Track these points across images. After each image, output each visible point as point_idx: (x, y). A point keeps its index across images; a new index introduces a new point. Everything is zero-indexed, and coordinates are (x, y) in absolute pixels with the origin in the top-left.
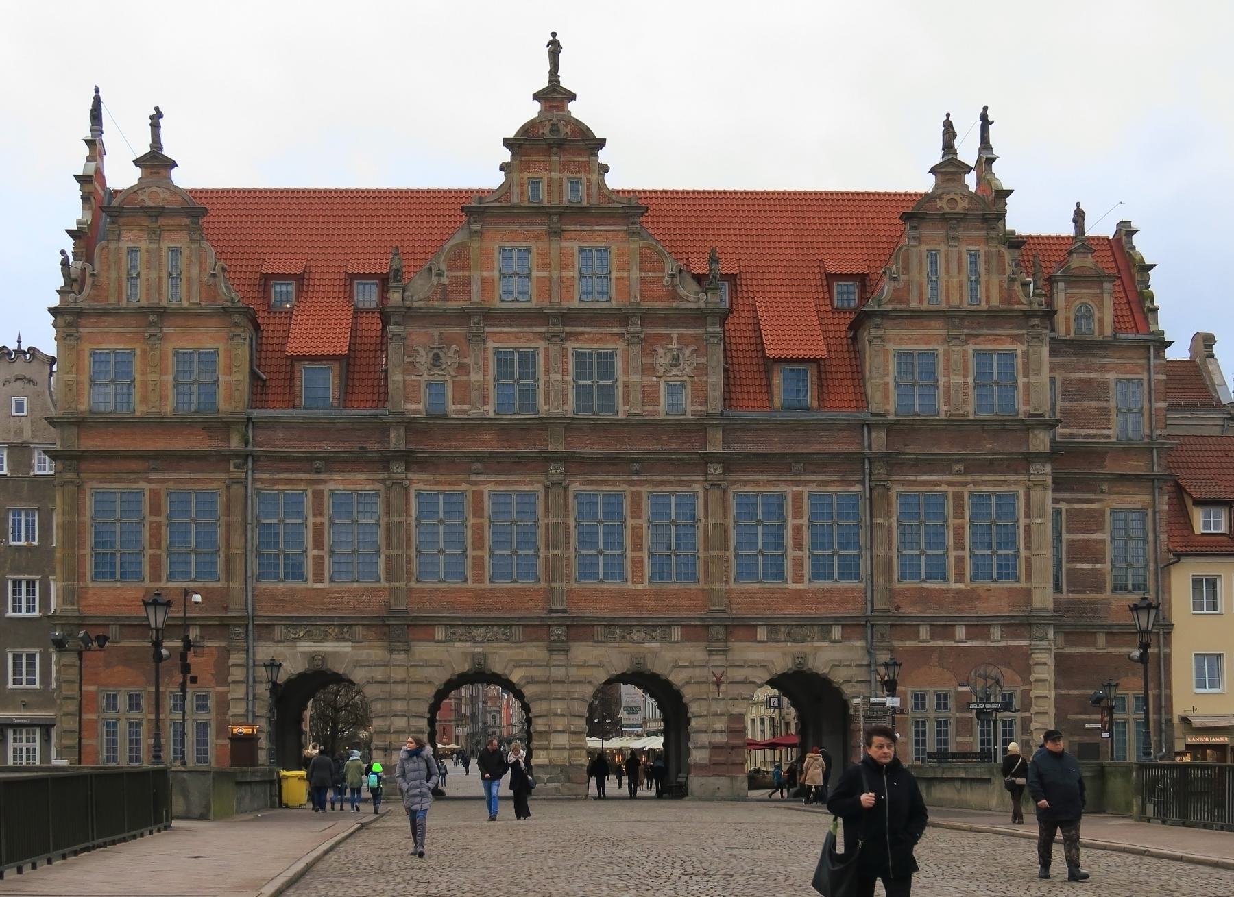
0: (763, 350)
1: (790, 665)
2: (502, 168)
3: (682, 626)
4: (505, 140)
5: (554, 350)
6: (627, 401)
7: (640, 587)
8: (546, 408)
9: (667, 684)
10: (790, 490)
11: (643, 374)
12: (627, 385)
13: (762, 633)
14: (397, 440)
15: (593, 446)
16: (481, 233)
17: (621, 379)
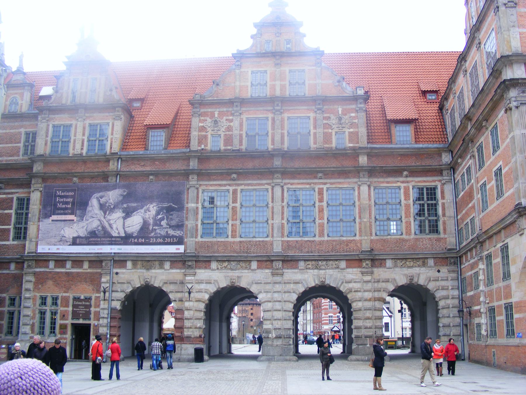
0: (386, 117)
1: (406, 282)
2: (252, 37)
3: (346, 260)
4: (254, 23)
5: (278, 118)
6: (315, 143)
7: (322, 239)
8: (272, 147)
9: (340, 292)
10: (402, 185)
11: (324, 129)
12: (315, 134)
13: (389, 263)
14: (194, 164)
15: (297, 164)
16: (240, 66)
17: (312, 131)
